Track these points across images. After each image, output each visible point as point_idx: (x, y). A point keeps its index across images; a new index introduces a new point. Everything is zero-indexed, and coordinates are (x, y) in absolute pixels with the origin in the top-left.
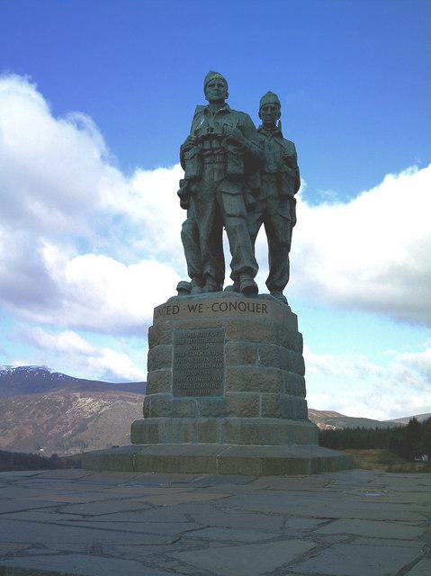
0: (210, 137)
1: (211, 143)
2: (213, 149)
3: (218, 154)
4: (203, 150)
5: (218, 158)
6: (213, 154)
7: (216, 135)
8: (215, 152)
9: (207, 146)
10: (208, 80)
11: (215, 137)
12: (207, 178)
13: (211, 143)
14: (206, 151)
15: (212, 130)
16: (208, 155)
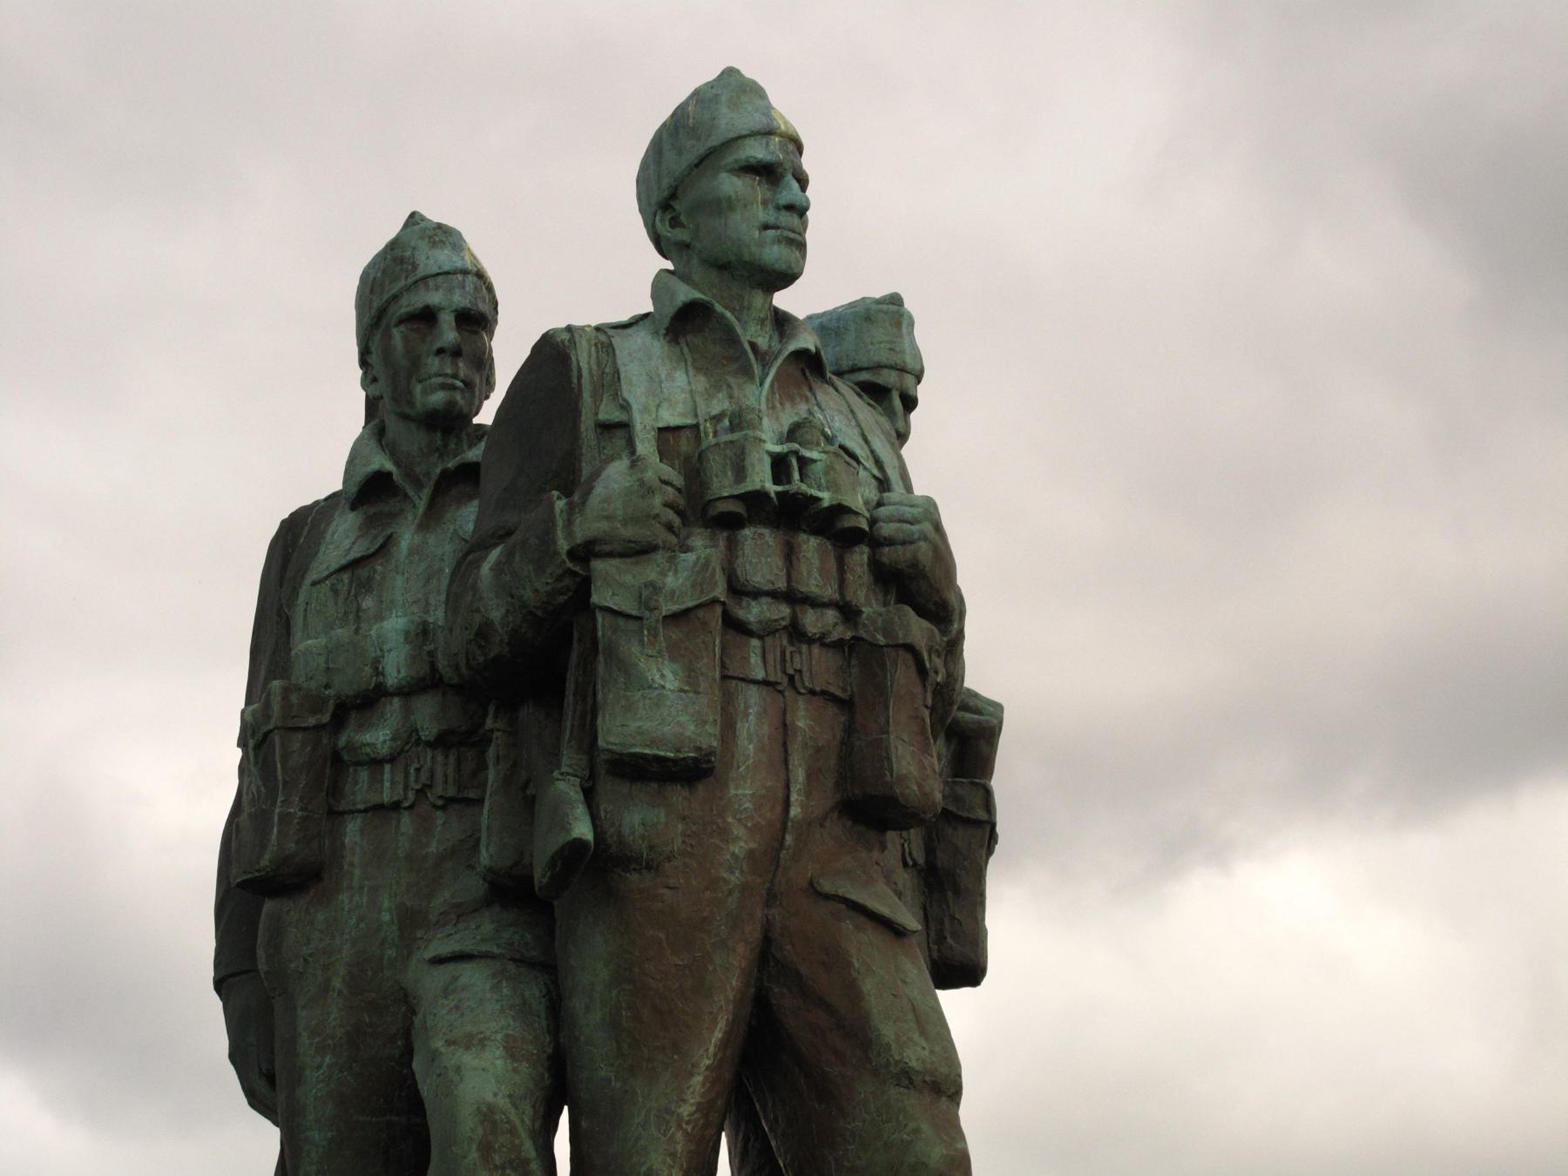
0: (792, 514)
1: (790, 555)
2: (791, 597)
3: (821, 640)
4: (739, 590)
5: (820, 667)
6: (796, 632)
7: (840, 510)
8: (812, 621)
9: (760, 557)
10: (730, 121)
11: (832, 525)
12: (745, 789)
13: (790, 555)
14: (756, 594)
15: (804, 462)
16: (767, 631)
